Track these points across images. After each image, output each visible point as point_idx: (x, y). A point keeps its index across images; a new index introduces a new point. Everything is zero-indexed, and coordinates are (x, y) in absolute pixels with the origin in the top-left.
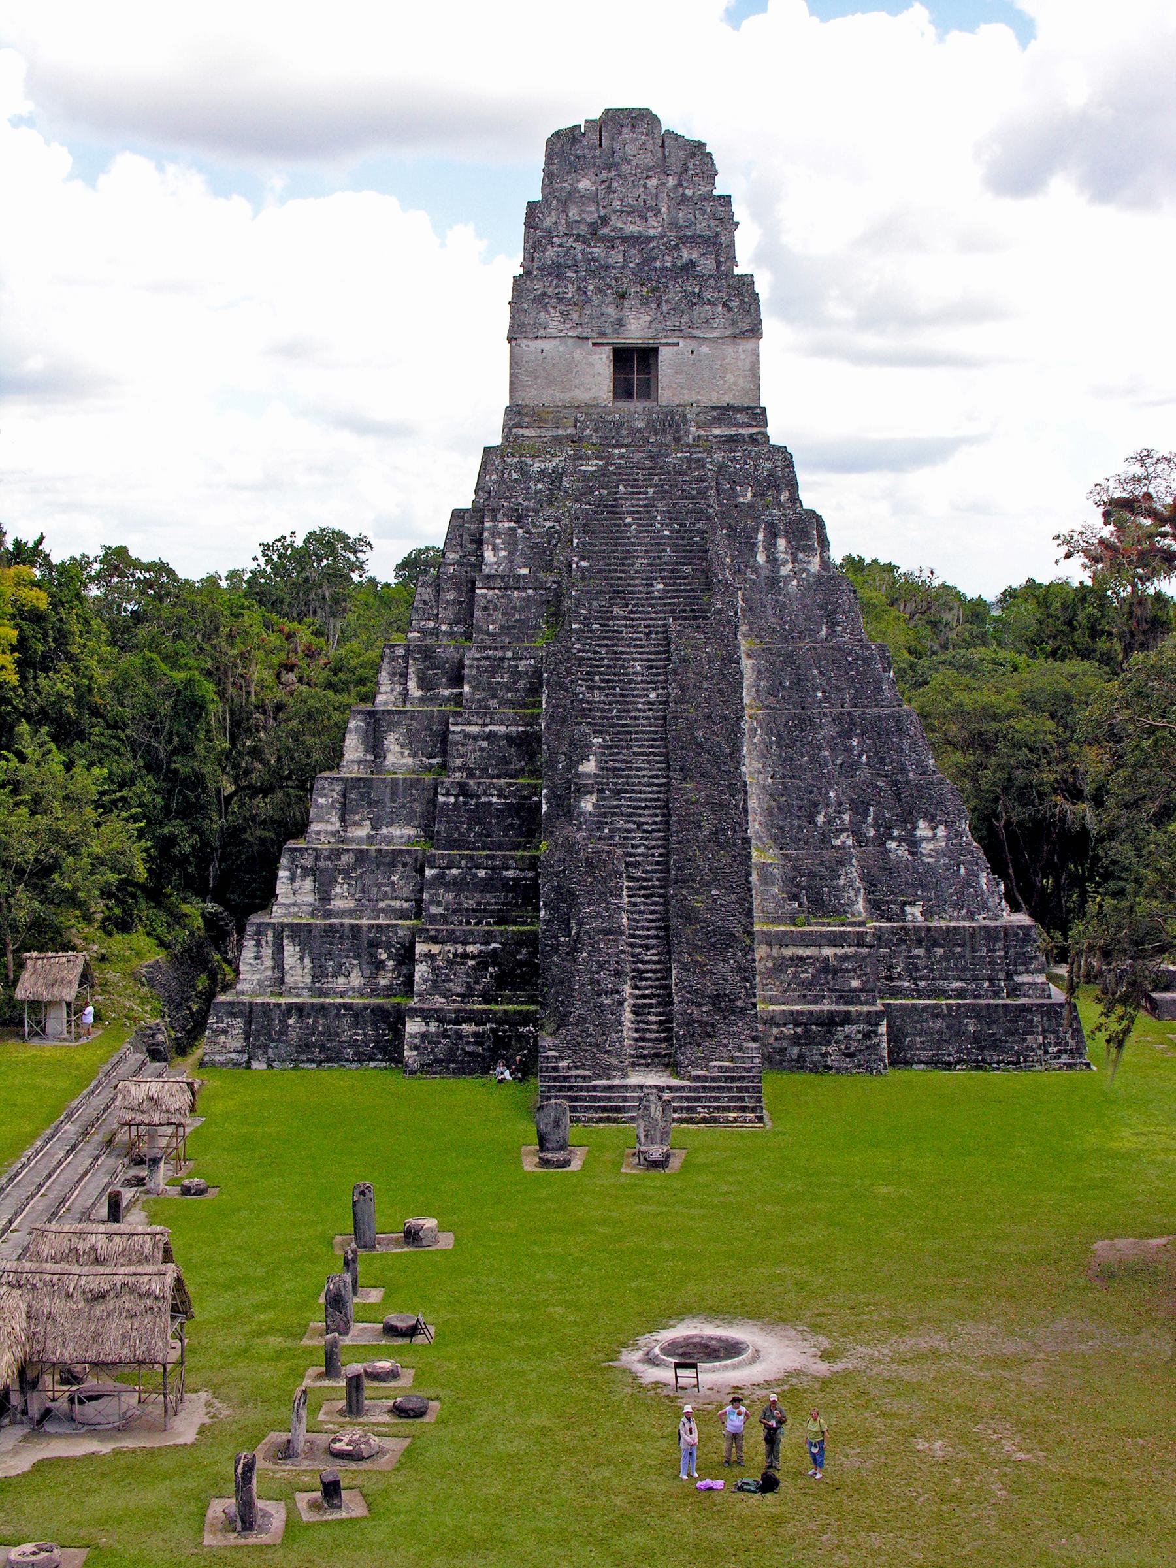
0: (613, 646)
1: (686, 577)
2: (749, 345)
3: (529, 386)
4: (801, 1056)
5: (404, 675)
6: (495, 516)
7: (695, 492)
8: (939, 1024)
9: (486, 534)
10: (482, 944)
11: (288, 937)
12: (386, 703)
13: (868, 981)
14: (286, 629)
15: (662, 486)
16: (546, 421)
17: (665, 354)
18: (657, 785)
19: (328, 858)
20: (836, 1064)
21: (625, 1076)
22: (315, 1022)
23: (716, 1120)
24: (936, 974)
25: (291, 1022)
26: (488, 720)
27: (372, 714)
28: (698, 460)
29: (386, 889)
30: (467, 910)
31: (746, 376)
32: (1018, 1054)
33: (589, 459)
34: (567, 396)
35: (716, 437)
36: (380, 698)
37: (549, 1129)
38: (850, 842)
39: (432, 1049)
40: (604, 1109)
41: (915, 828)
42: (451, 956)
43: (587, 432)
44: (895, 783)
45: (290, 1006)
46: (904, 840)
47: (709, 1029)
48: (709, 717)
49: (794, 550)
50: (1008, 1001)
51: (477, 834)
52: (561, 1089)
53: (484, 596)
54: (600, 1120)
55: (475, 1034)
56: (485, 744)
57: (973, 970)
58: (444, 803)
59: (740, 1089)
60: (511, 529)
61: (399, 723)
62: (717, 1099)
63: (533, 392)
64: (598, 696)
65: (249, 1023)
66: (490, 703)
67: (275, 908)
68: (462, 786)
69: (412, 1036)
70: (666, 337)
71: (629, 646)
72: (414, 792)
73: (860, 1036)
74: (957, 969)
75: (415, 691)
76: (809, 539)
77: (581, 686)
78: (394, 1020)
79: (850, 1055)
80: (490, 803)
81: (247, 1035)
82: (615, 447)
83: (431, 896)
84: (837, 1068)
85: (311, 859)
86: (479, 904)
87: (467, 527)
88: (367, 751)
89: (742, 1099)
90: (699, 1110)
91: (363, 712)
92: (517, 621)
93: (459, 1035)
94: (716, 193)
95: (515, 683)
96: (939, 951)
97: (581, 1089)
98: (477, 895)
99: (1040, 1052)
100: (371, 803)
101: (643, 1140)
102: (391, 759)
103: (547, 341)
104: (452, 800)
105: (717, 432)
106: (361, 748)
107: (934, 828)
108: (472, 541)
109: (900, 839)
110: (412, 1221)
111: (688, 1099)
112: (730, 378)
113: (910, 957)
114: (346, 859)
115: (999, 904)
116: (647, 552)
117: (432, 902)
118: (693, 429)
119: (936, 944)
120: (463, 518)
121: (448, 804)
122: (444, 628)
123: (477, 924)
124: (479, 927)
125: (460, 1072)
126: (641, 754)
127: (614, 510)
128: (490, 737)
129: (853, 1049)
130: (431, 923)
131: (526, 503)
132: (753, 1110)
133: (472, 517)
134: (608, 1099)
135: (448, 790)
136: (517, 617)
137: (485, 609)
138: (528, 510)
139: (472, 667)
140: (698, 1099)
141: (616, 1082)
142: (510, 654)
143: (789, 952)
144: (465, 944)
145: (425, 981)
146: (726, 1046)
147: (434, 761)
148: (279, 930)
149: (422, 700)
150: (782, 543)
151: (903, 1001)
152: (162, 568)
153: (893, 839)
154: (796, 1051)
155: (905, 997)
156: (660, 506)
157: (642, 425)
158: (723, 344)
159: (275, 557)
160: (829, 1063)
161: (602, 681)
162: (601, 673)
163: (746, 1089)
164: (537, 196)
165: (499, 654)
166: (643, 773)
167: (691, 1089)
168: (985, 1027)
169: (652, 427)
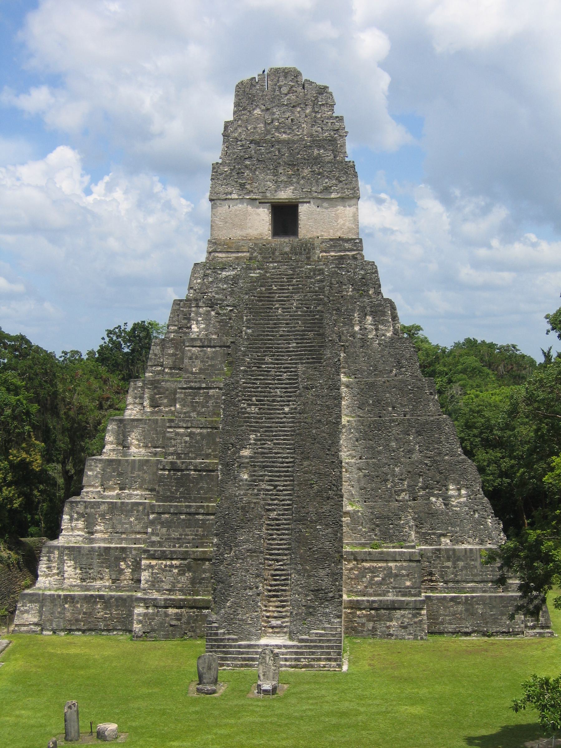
0: (264, 379)
1: (310, 339)
3: (222, 227)
4: (374, 629)
5: (142, 398)
6: (198, 304)
7: (317, 289)
8: (460, 608)
9: (192, 315)
10: (182, 559)
11: (67, 554)
12: (130, 415)
13: (415, 582)
14: (104, 377)
15: (298, 285)
16: (230, 248)
17: (302, 209)
18: (287, 463)
19: (92, 507)
20: (395, 633)
21: (259, 639)
22: (81, 606)
23: (312, 666)
24: (459, 578)
25: (66, 606)
26: (189, 425)
27: (121, 421)
28: (320, 270)
29: (127, 526)
30: (174, 538)
31: (350, 220)
32: (509, 626)
33: (255, 269)
34: (243, 233)
35: (332, 256)
36: (128, 412)
37: (205, 670)
38: (407, 497)
39: (150, 623)
40: (244, 659)
41: (447, 490)
42: (163, 567)
43: (255, 254)
44: (435, 461)
45: (66, 596)
46: (441, 496)
47: (311, 610)
48: (320, 421)
49: (376, 324)
50: (503, 594)
51: (181, 493)
52: (218, 647)
53: (189, 351)
54: (242, 666)
55: (176, 614)
56: (188, 439)
57: (482, 575)
58: (162, 474)
59: (328, 647)
60: (207, 311)
61: (137, 427)
62: (313, 653)
63: (224, 231)
64: (253, 409)
65: (41, 607)
66: (192, 414)
67: (60, 538)
68: (171, 463)
69: (139, 615)
70: (303, 198)
71: (274, 380)
72: (145, 468)
73: (410, 616)
74: (472, 575)
76: (385, 316)
77: (244, 404)
78: (127, 604)
79: (405, 628)
80: (189, 475)
81: (40, 612)
82: (271, 262)
83: (153, 530)
84: (396, 635)
85: (83, 508)
86: (181, 535)
87: (182, 311)
88: (118, 444)
89: (329, 653)
90: (302, 660)
91: (116, 420)
92: (209, 366)
93: (167, 615)
94: (334, 115)
95: (207, 402)
96: (461, 564)
97: (231, 647)
98: (180, 530)
99: (523, 626)
100: (120, 475)
101: (262, 677)
103: (231, 201)
105: (333, 254)
107: (459, 490)
108: (185, 319)
109: (437, 496)
110: (102, 726)
111: (296, 653)
112: (341, 221)
113: (443, 567)
114: (103, 508)
115: (499, 535)
116: (287, 324)
117: (153, 534)
118: (318, 252)
119: (459, 559)
120: (179, 304)
121: (164, 475)
122: (166, 370)
123: (179, 547)
124: (182, 549)
125: (167, 637)
126: (279, 444)
127: (270, 299)
129: (406, 623)
130: (152, 547)
131: (217, 296)
132: (336, 660)
133: (185, 304)
134: (247, 653)
135: (164, 466)
136: (210, 363)
137: (191, 358)
138: (217, 300)
139: (181, 393)
140: (302, 653)
141: (252, 643)
142: (204, 385)
143: (367, 565)
144: (172, 559)
145: (147, 581)
146: (321, 621)
148: (62, 550)
149: (152, 413)
150: (369, 319)
151: (438, 595)
152: (22, 338)
153: (434, 495)
154: (370, 625)
155: (441, 592)
156: (296, 297)
157: (287, 249)
158: (336, 201)
159: (115, 338)
160: (391, 632)
161: (257, 400)
162: (256, 396)
163: (332, 647)
164: (231, 118)
165: (197, 385)
166: (279, 455)
167: (298, 647)
168: (488, 611)
169: (294, 250)
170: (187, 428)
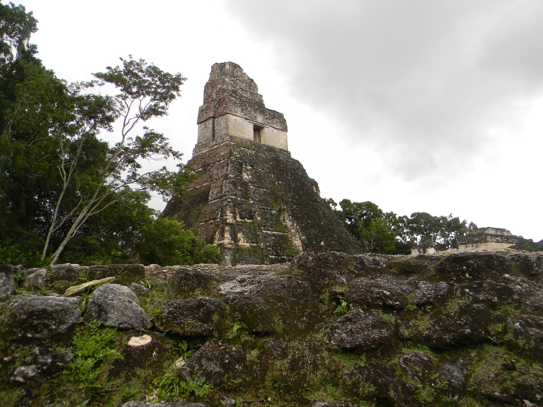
2: (285, 133)
17: (266, 129)
56: (273, 238)
75: (238, 219)
102: (240, 243)
104: (274, 257)
106: (230, 238)
108: (238, 172)
128: (274, 235)
147: (254, 245)
170: (272, 231)
